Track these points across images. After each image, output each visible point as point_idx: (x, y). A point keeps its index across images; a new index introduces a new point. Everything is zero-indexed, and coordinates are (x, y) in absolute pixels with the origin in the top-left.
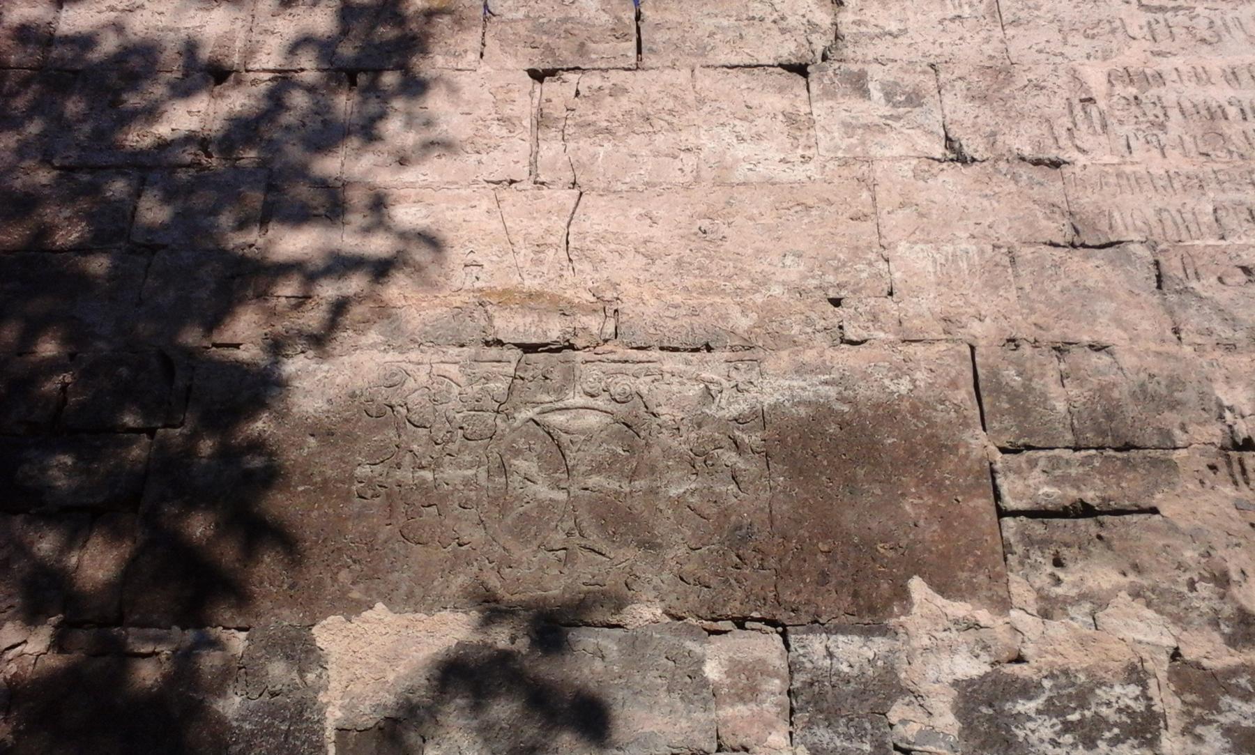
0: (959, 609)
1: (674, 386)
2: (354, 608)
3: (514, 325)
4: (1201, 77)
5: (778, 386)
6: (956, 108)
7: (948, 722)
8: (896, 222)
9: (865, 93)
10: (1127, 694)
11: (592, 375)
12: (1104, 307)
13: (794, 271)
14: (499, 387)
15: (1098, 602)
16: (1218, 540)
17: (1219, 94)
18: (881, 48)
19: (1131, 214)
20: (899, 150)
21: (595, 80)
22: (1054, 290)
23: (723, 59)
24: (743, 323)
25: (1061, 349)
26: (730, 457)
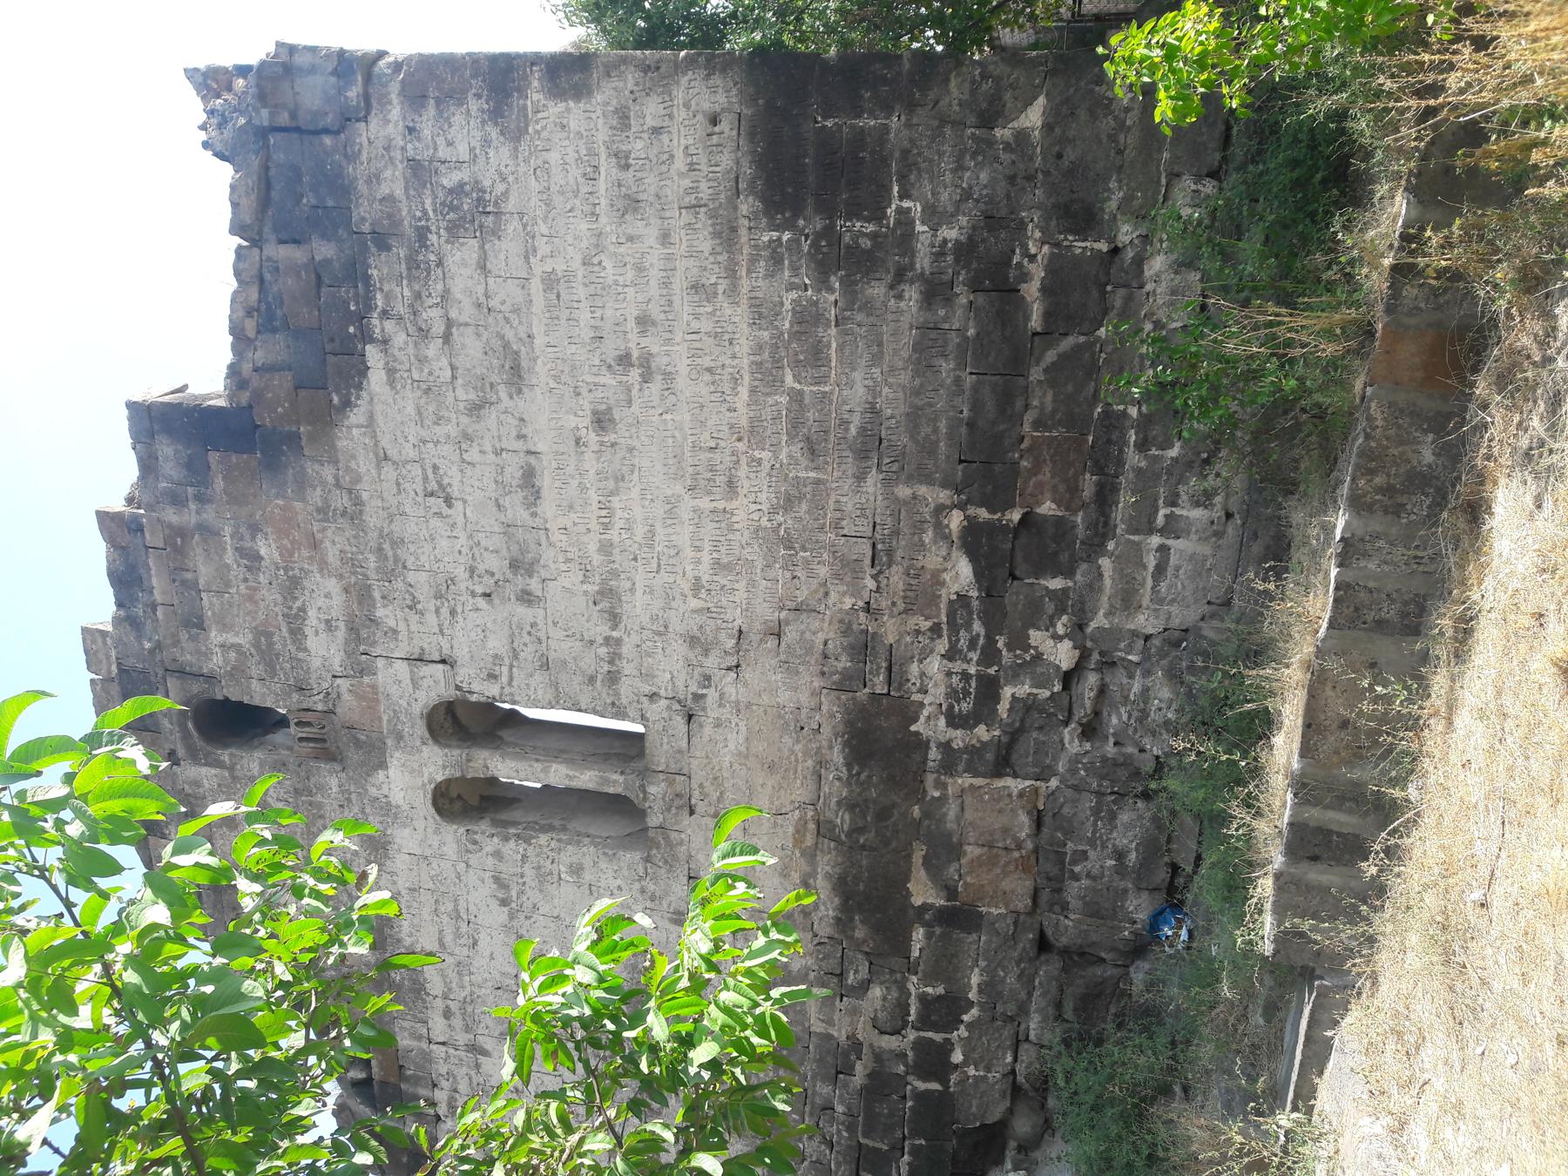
0: (922, 719)
1: (834, 788)
2: (909, 894)
3: (809, 840)
4: (698, 562)
5: (837, 756)
6: (712, 662)
7: (959, 732)
8: (766, 699)
9: (703, 696)
10: (955, 679)
11: (829, 815)
12: (808, 635)
13: (788, 740)
14: (832, 844)
15: (923, 674)
16: (903, 628)
17: (706, 558)
18: (680, 684)
19: (766, 612)
20: (733, 690)
21: (696, 794)
22: (799, 652)
23: (684, 744)
24: (810, 763)
25: (826, 657)
26: (863, 776)
